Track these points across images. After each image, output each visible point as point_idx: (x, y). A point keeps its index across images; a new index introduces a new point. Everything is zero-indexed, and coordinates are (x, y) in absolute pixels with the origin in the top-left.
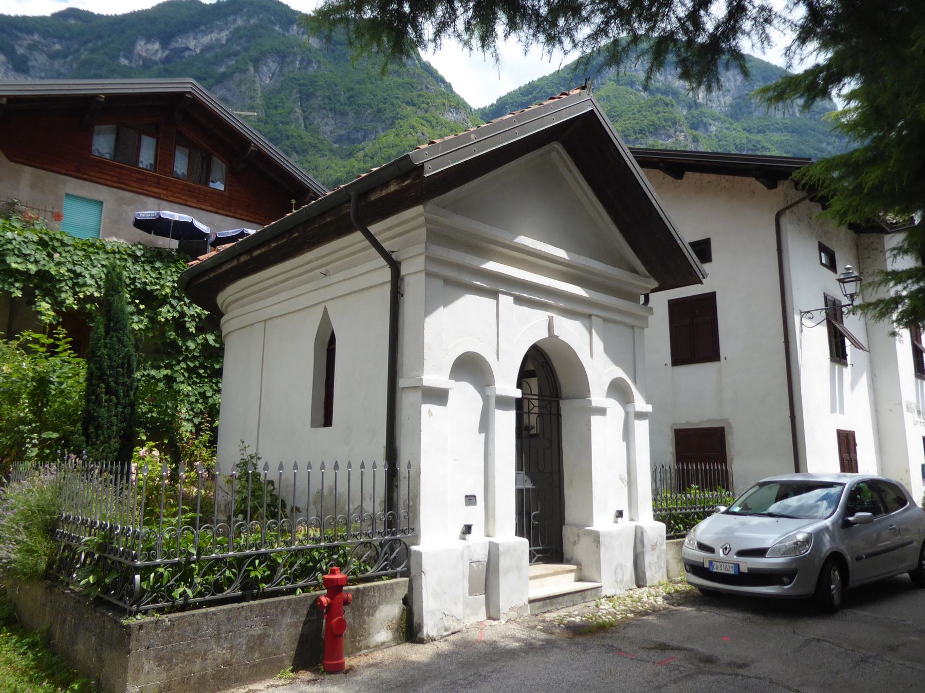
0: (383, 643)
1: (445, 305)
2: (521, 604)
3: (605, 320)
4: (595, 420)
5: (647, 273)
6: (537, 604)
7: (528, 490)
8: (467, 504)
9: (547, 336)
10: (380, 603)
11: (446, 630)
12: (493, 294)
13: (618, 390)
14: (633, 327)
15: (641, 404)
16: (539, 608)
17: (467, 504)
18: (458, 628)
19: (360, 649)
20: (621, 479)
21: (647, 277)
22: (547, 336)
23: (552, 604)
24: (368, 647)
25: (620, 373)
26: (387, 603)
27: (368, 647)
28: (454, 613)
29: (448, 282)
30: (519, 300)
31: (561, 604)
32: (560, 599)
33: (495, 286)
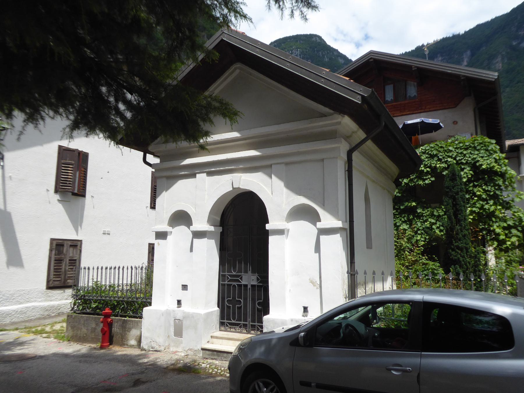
0: (133, 345)
1: (167, 190)
2: (196, 349)
3: (287, 164)
4: (272, 239)
5: (331, 111)
6: (207, 352)
7: (253, 286)
8: (183, 290)
9: (231, 189)
10: (132, 328)
11: (152, 348)
12: (194, 176)
13: (301, 213)
14: (323, 160)
15: (328, 221)
16: (209, 355)
17: (183, 290)
18: (158, 349)
19: (124, 345)
20: (312, 282)
21: (331, 114)
22: (231, 189)
23: (218, 356)
24: (127, 345)
25: (303, 200)
26: (135, 329)
27: (127, 345)
28: (157, 341)
29: (169, 178)
30: (210, 174)
31: (225, 357)
32: (225, 355)
33: (192, 172)
